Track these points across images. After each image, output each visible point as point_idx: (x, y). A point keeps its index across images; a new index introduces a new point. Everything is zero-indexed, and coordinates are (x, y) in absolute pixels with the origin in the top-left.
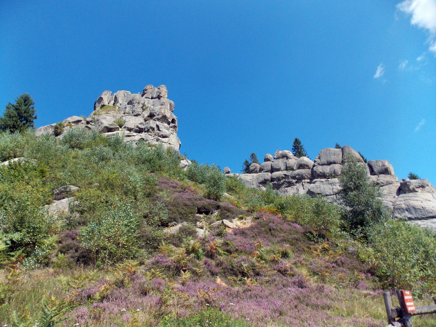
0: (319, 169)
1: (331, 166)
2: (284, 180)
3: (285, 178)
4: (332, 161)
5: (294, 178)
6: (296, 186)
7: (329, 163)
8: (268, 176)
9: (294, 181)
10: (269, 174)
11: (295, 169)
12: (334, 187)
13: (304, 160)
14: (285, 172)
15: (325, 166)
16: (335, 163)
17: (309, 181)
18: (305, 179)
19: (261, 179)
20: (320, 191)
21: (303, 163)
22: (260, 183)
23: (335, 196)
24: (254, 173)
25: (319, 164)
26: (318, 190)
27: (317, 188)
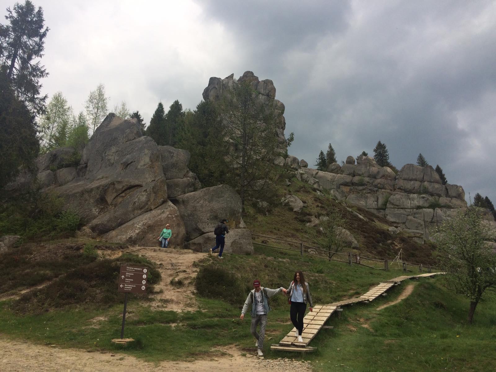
0: (401, 183)
1: (412, 182)
2: (366, 187)
3: (366, 185)
4: (414, 178)
5: (376, 186)
6: (376, 194)
7: (411, 180)
8: (348, 179)
9: (376, 189)
10: (351, 177)
11: (377, 178)
12: (412, 202)
13: (387, 171)
14: (367, 179)
15: (406, 181)
16: (416, 180)
17: (389, 191)
18: (385, 189)
19: (341, 182)
20: (400, 203)
21: (386, 173)
22: (342, 185)
23: (411, 210)
25: (401, 178)
26: (398, 202)
27: (397, 200)
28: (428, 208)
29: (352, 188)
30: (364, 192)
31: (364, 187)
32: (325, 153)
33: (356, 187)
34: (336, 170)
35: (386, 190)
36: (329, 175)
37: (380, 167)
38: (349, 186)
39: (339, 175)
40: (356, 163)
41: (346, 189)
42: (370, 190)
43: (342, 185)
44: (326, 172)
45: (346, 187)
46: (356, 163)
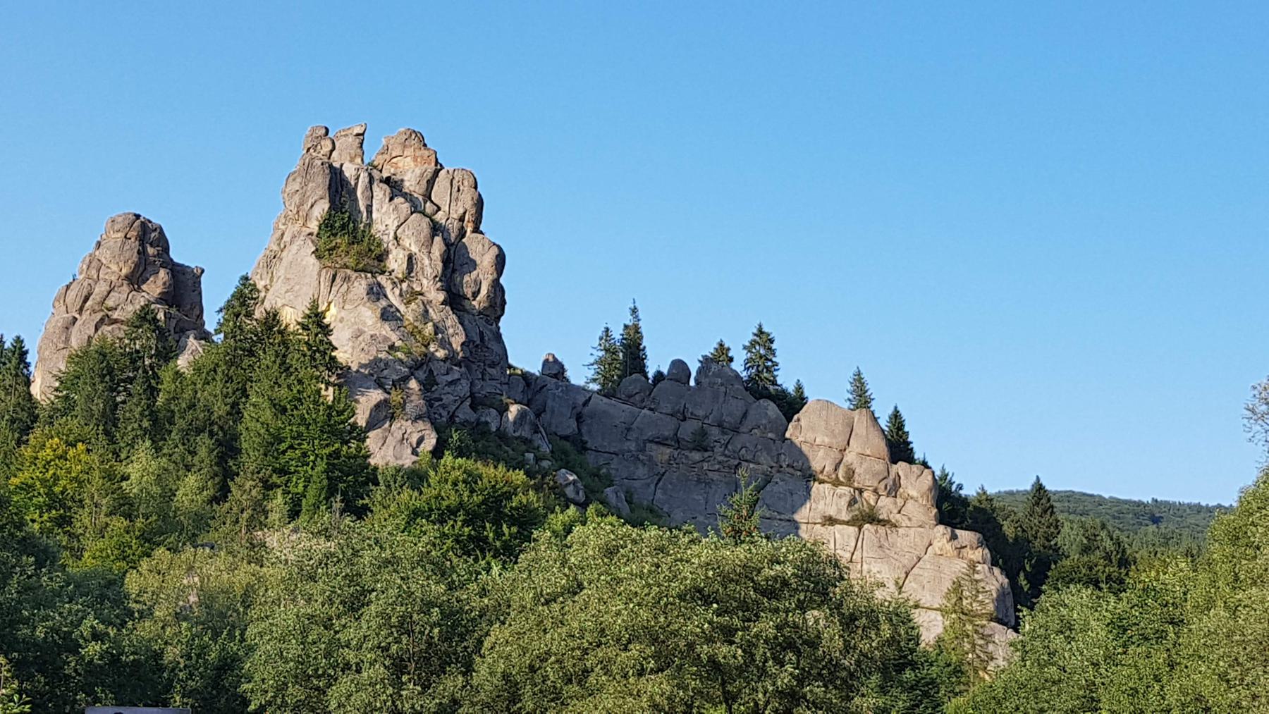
19: (649, 434)
24: (633, 404)
29: (676, 453)
30: (705, 466)
31: (706, 454)
33: (687, 453)
34: (637, 397)
35: (760, 467)
38: (669, 446)
39: (645, 411)
40: (692, 383)
41: (662, 454)
42: (720, 463)
43: (651, 441)
44: (613, 401)
45: (663, 449)
46: (692, 383)
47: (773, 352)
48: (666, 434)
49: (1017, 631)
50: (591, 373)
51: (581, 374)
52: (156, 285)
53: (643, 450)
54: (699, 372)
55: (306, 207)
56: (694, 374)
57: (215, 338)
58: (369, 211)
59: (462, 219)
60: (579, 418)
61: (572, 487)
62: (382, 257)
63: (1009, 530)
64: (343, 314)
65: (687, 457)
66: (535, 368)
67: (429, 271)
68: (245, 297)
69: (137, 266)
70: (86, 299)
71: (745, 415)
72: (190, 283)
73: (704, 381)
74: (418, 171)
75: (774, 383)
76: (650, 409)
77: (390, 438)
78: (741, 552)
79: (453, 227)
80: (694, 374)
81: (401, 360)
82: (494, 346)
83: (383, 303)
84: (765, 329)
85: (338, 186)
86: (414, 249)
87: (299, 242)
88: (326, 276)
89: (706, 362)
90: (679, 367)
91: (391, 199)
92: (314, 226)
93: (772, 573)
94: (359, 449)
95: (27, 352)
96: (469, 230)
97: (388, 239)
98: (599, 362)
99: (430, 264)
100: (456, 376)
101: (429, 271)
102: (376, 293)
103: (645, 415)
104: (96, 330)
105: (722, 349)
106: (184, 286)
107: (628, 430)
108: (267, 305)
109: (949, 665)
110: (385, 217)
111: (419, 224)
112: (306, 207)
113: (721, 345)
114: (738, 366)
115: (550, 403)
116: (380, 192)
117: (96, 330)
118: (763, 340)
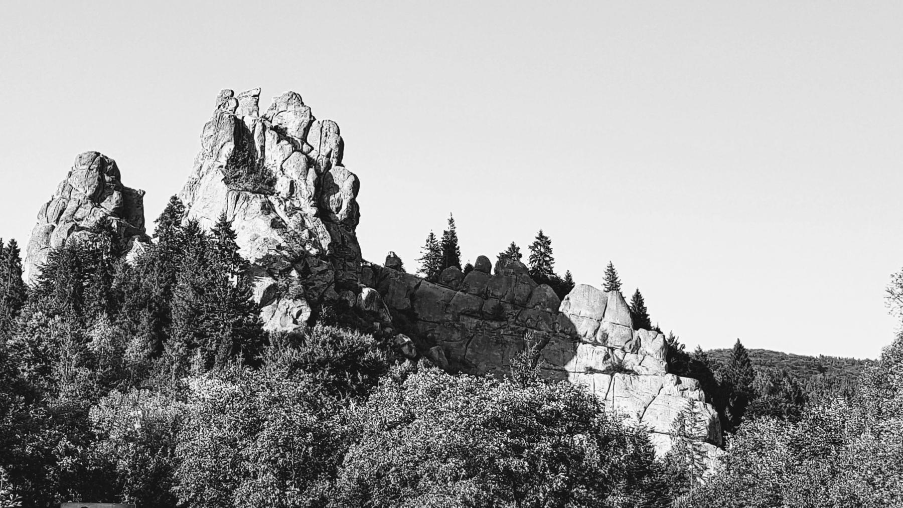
18: (540, 330)
28: (603, 372)
31: (502, 324)
32: (439, 238)
35: (541, 332)
36: (441, 292)
37: (534, 284)
38: (476, 317)
40: (493, 273)
41: (471, 323)
42: (512, 329)
43: (463, 314)
46: (493, 273)
47: (550, 251)
48: (474, 308)
49: (723, 449)
50: (420, 266)
51: (414, 266)
52: (111, 203)
53: (457, 321)
54: (498, 264)
55: (218, 147)
56: (494, 266)
57: (153, 241)
58: (263, 148)
59: (329, 156)
60: (412, 297)
61: (407, 347)
62: (273, 182)
63: (718, 376)
64: (244, 223)
65: (489, 325)
66: (381, 262)
67: (305, 192)
68: (174, 210)
69: (97, 189)
70: (61, 213)
71: (530, 295)
72: (135, 201)
73: (501, 271)
74: (297, 122)
75: (551, 272)
76: (462, 291)
77: (277, 311)
78: (527, 393)
79: (322, 162)
80: (494, 266)
81: (285, 256)
82: (352, 247)
83: (273, 216)
84: (544, 234)
85: (241, 133)
86: (295, 177)
87: (212, 172)
88: (232, 196)
89: (503, 257)
90: (483, 261)
91: (278, 142)
92: (223, 161)
93: (550, 408)
94: (255, 319)
95: (19, 250)
96: (334, 162)
97: (276, 171)
98: (427, 257)
99: (306, 188)
100: (325, 268)
101: (305, 192)
102: (267, 208)
103: (459, 295)
104: (69, 235)
105: (514, 248)
106: (131, 203)
107: (447, 305)
108: (190, 217)
109: (675, 473)
110: (274, 154)
111: (298, 160)
112: (218, 147)
113: (513, 246)
114: (525, 260)
115: (391, 286)
116: (271, 136)
117: (69, 235)
118: (543, 241)
